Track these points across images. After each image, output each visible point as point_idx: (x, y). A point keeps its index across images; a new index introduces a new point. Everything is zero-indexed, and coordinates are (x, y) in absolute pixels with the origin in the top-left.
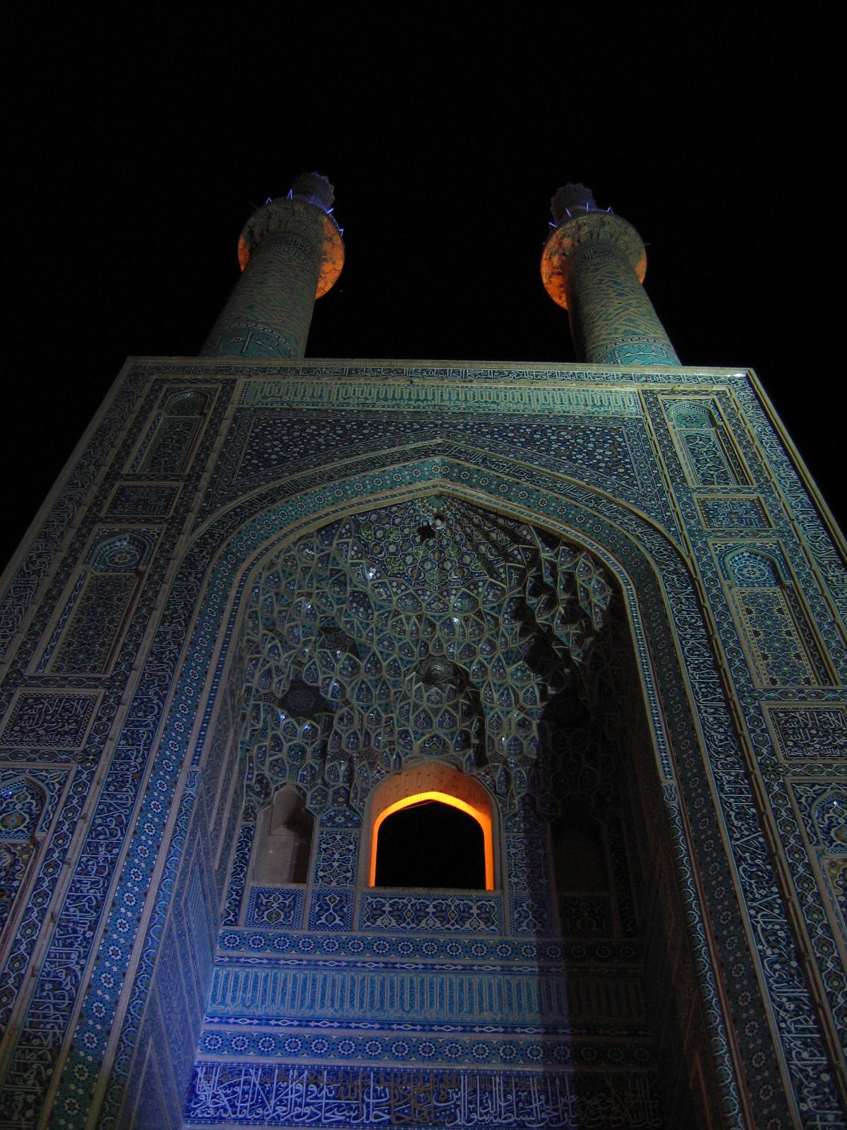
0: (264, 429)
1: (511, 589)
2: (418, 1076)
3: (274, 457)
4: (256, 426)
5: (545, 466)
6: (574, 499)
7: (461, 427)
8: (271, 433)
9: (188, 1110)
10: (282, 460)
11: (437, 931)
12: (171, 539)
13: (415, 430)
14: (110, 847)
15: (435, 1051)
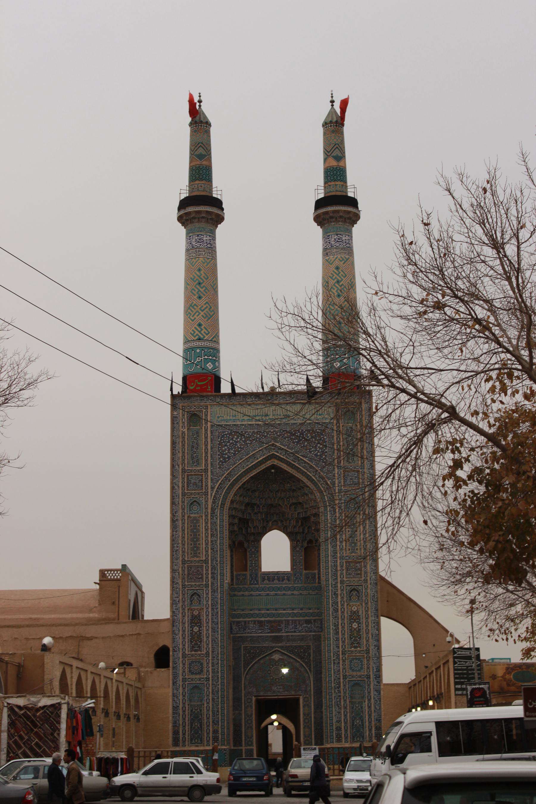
0: (221, 440)
1: (294, 486)
2: (275, 621)
3: (226, 456)
4: (219, 437)
5: (302, 456)
6: (310, 472)
7: (278, 434)
8: (224, 442)
9: (231, 632)
10: (229, 458)
11: (277, 584)
12: (207, 501)
13: (265, 437)
14: (217, 608)
15: (279, 615)
